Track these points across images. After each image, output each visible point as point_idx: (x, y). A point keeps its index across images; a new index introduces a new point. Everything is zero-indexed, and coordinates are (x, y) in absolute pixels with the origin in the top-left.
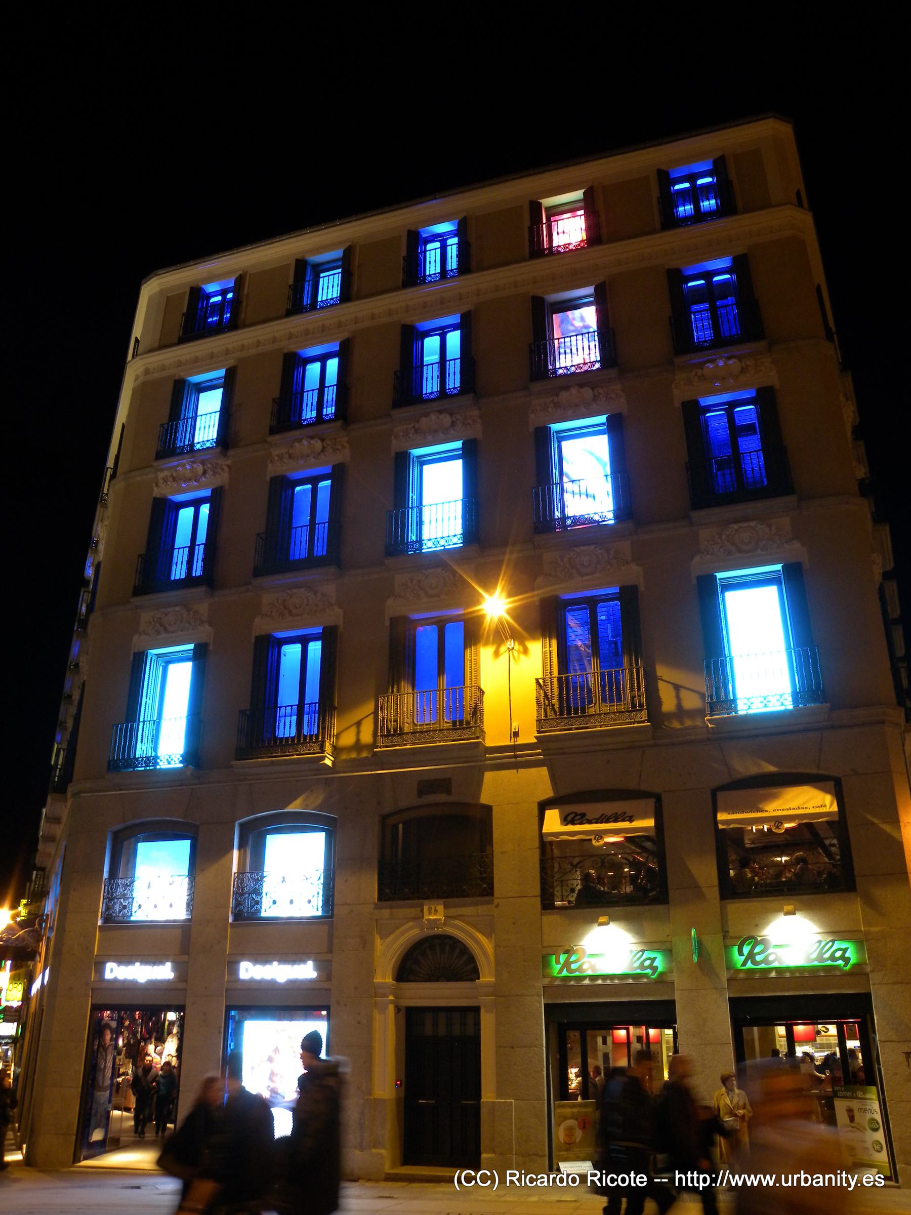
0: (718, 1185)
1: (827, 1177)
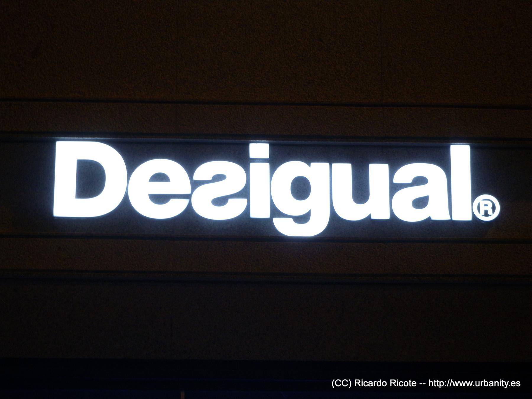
0: (447, 386)
1: (495, 382)
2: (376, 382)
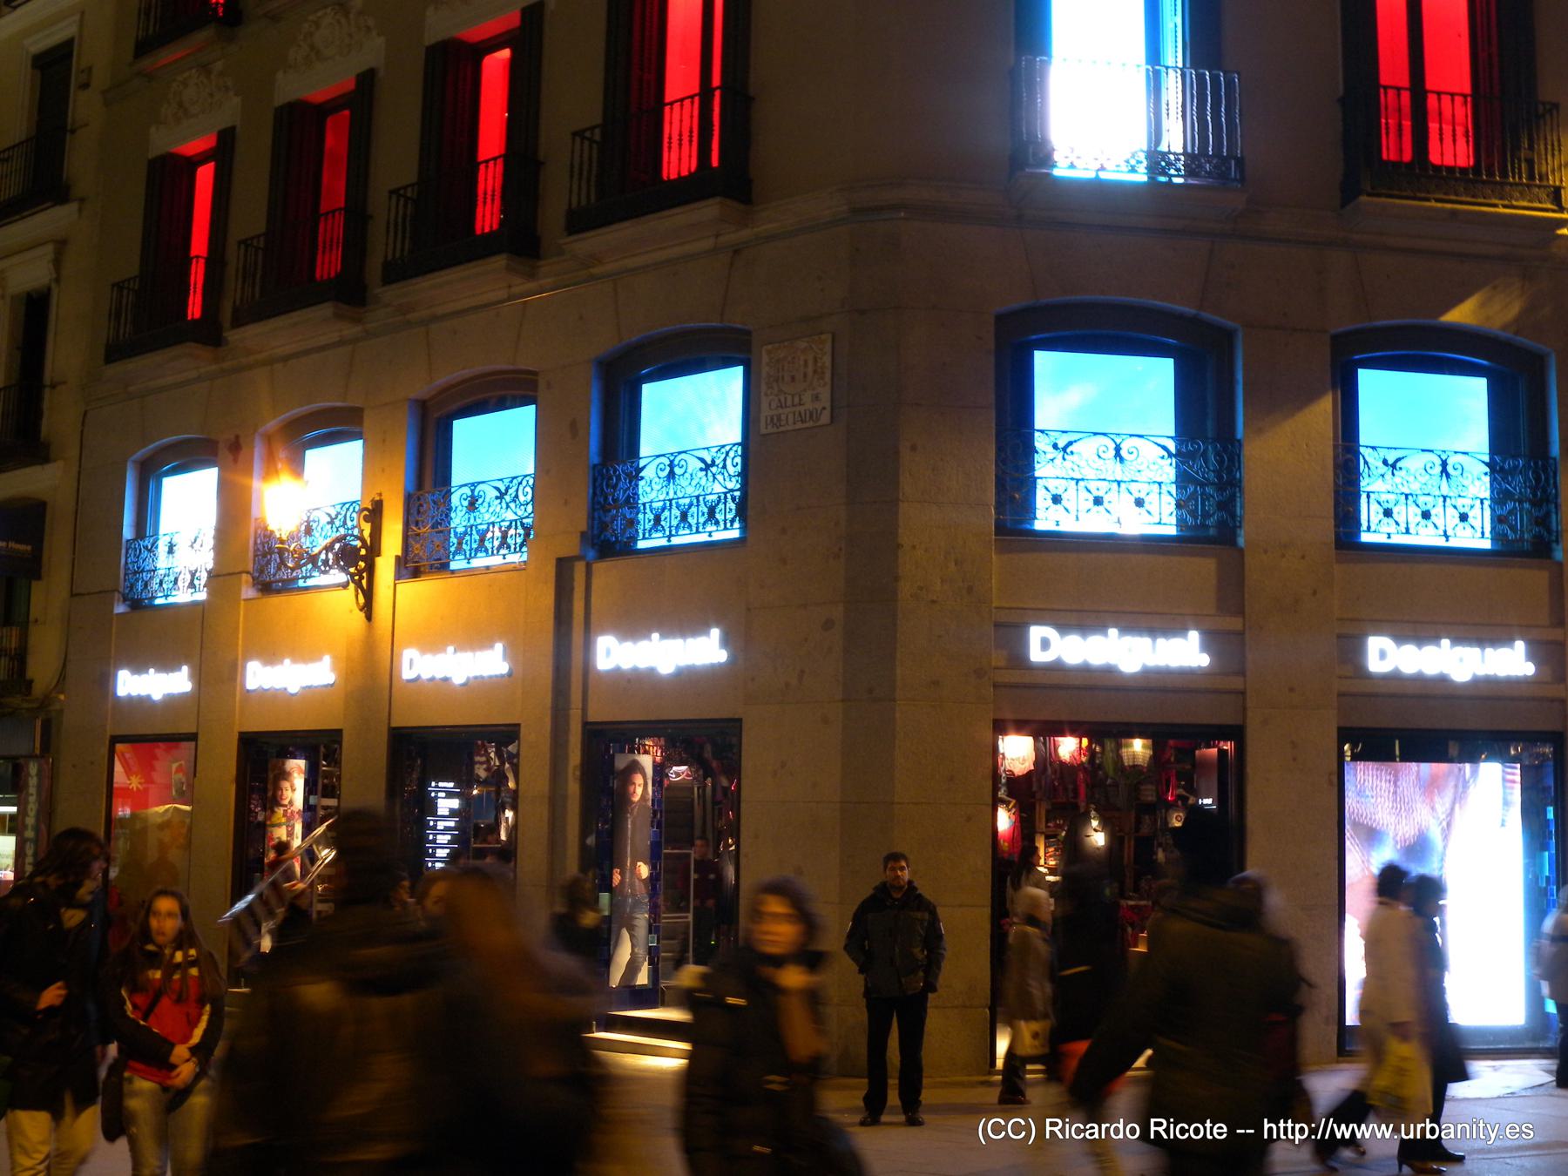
0: (1319, 1137)
2: (1108, 1125)
